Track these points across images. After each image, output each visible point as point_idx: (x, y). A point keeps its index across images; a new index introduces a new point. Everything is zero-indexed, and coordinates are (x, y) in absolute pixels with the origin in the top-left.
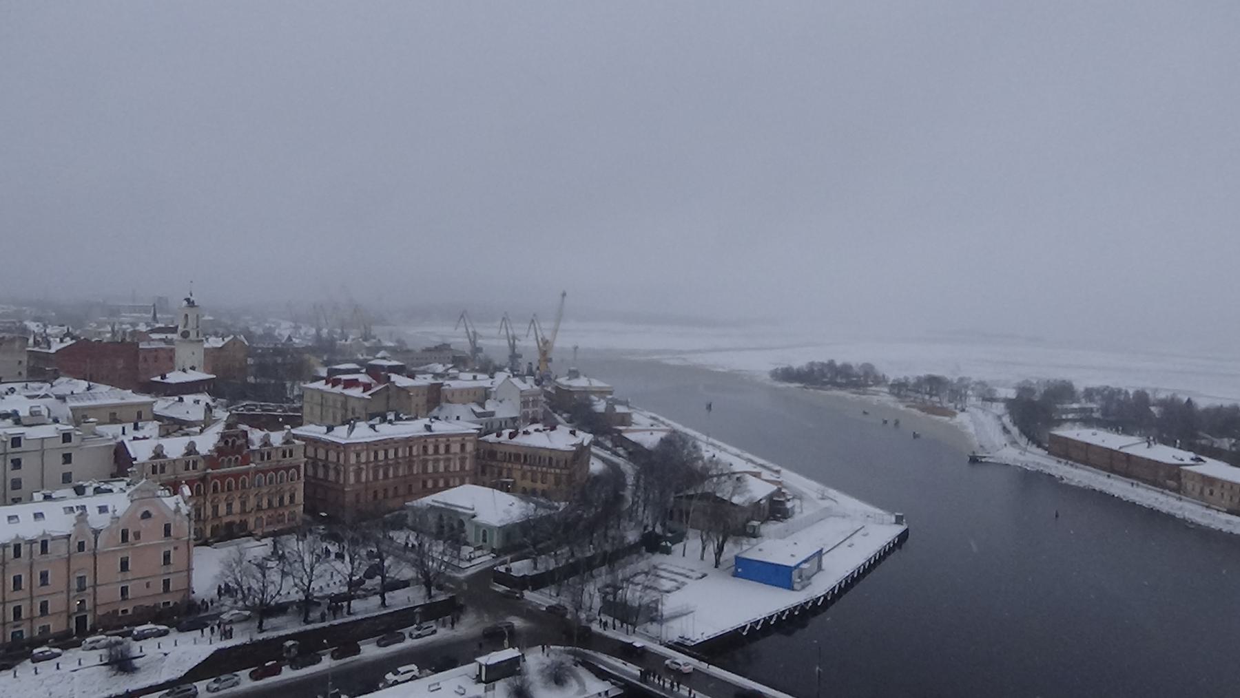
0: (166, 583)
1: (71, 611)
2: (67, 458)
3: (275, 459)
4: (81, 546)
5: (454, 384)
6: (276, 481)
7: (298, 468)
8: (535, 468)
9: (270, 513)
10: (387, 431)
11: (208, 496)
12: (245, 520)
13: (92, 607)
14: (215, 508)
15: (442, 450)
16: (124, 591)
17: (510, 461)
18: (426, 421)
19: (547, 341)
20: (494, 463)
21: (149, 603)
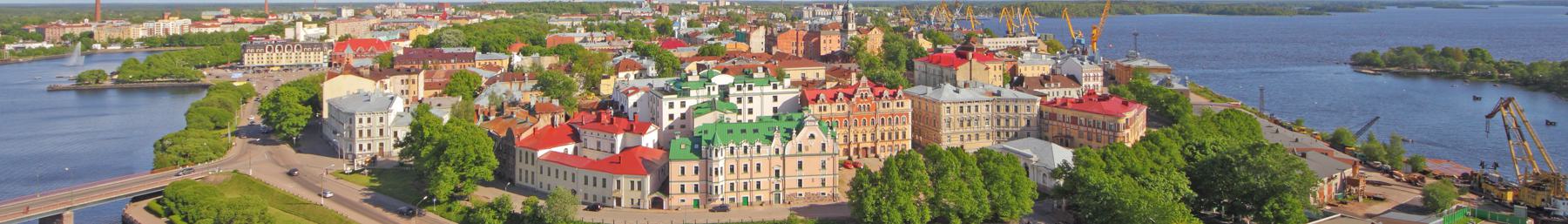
2: (775, 99)
4: (777, 151)
7: (907, 115)
9: (890, 143)
15: (1012, 109)
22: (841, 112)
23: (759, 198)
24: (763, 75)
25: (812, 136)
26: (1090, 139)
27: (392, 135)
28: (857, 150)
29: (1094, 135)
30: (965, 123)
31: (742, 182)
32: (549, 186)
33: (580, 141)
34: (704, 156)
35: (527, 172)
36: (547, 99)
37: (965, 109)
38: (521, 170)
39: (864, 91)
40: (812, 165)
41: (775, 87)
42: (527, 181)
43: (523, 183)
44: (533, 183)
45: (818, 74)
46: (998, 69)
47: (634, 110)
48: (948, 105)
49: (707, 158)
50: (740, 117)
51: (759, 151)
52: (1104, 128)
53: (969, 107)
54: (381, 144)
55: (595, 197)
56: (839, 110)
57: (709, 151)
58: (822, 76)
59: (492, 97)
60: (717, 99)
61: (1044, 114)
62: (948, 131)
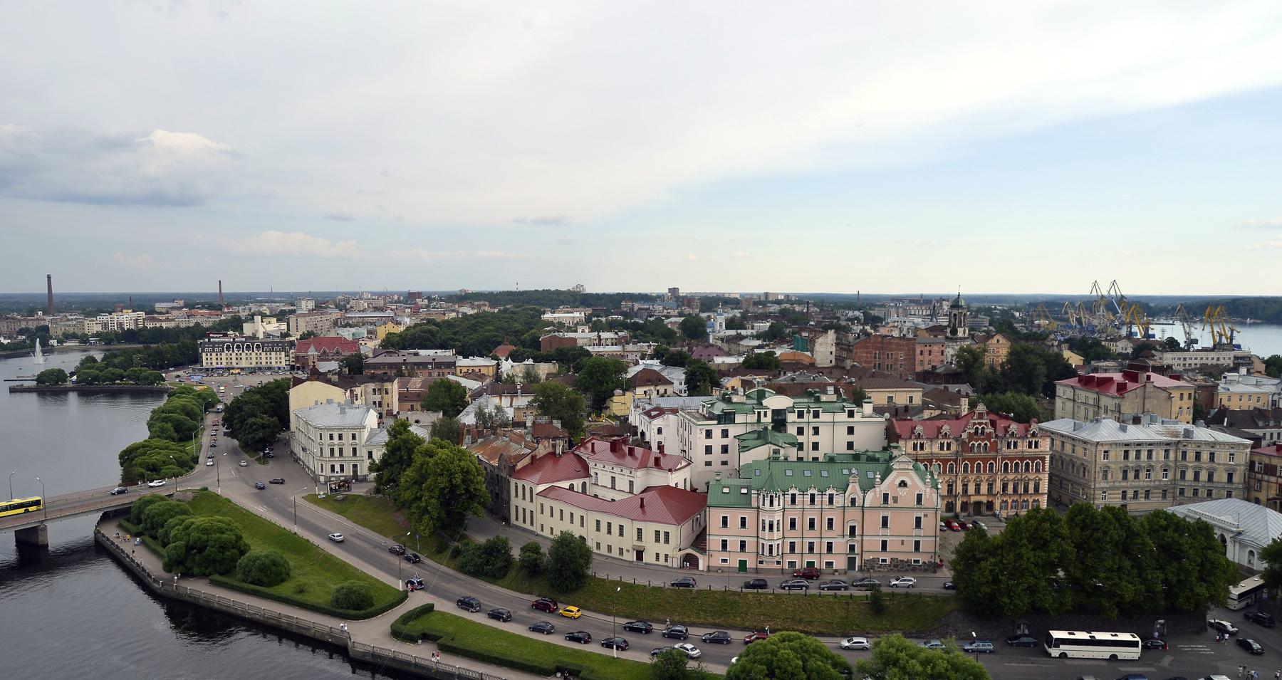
0: (917, 544)
2: (851, 431)
3: (1020, 449)
4: (853, 501)
5: (1235, 389)
7: (1043, 459)
10: (1135, 433)
12: (992, 501)
14: (965, 486)
15: (1205, 456)
16: (884, 544)
18: (1190, 427)
20: (1273, 479)
22: (945, 451)
23: (829, 564)
24: (834, 398)
27: (366, 455)
28: (965, 506)
30: (1131, 475)
31: (807, 541)
32: (552, 529)
33: (589, 475)
34: (754, 504)
35: (524, 510)
36: (544, 419)
37: (1132, 455)
38: (517, 507)
39: (980, 424)
40: (902, 524)
41: (851, 414)
42: (524, 521)
43: (520, 523)
44: (532, 524)
45: (911, 399)
46: (1186, 396)
47: (660, 438)
48: (1106, 448)
49: (758, 508)
50: (801, 454)
53: (1138, 452)
54: (355, 466)
55: (610, 548)
56: (942, 449)
57: (761, 497)
58: (918, 399)
59: (480, 414)
60: (770, 428)
61: (1257, 465)
62: (1104, 485)
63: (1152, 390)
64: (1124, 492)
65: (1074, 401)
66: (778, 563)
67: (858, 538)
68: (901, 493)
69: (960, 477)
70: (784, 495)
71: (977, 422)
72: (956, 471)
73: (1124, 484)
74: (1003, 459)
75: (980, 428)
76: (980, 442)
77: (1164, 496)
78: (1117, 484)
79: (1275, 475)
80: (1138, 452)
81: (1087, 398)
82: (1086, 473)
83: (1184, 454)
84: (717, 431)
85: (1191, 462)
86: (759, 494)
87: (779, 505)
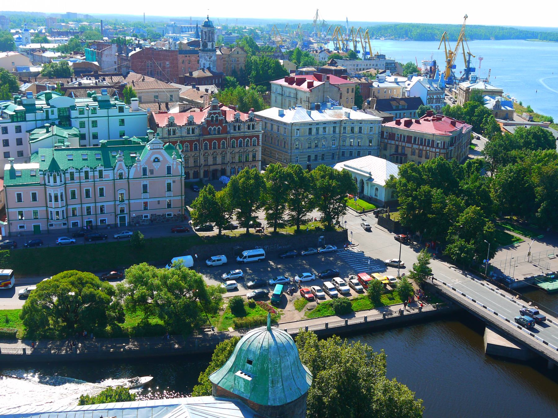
1: (117, 213)
6: (244, 145)
7: (258, 137)
8: (421, 147)
10: (317, 116)
11: (202, 151)
12: (225, 168)
13: (128, 212)
15: (356, 130)
17: (404, 141)
18: (348, 110)
19: (452, 53)
20: (393, 142)
21: (159, 213)
25: (157, 160)
26: (420, 156)
28: (206, 173)
29: (417, 151)
46: (350, 90)
49: (45, 185)
51: (101, 176)
52: (432, 146)
53: (317, 129)
56: (188, 133)
57: (46, 177)
61: (385, 134)
63: (328, 86)
64: (309, 156)
65: (282, 95)
66: (64, 224)
67: (126, 202)
68: (155, 167)
69: (202, 152)
70: (64, 173)
71: (212, 112)
72: (199, 149)
73: (309, 150)
74: (231, 138)
75: (215, 116)
76: (215, 127)
77: (333, 158)
78: (304, 151)
79: (394, 140)
80: (317, 129)
81: (290, 93)
82: (286, 145)
83: (345, 128)
84: (12, 127)
85: (348, 134)
86: (45, 174)
87: (61, 181)
